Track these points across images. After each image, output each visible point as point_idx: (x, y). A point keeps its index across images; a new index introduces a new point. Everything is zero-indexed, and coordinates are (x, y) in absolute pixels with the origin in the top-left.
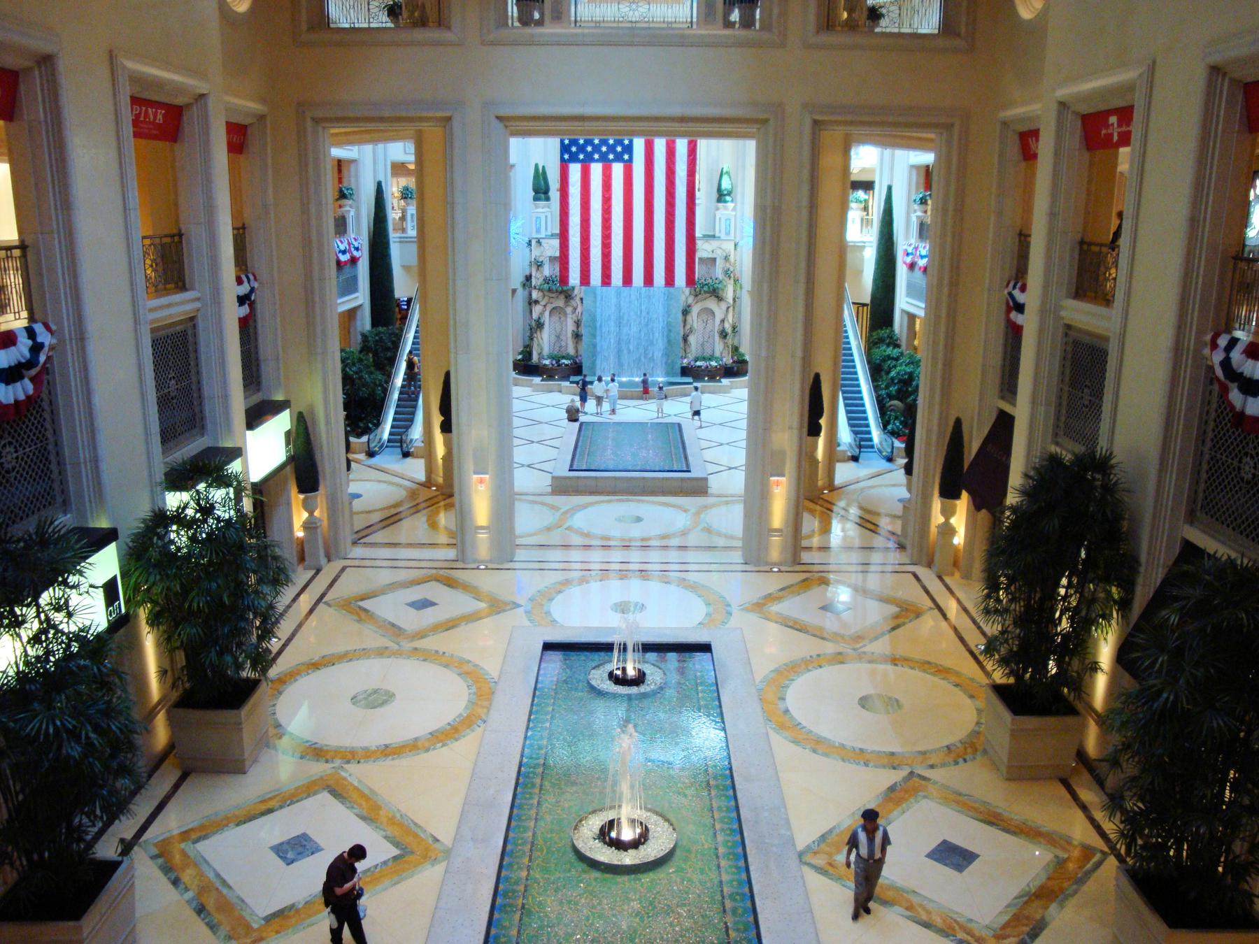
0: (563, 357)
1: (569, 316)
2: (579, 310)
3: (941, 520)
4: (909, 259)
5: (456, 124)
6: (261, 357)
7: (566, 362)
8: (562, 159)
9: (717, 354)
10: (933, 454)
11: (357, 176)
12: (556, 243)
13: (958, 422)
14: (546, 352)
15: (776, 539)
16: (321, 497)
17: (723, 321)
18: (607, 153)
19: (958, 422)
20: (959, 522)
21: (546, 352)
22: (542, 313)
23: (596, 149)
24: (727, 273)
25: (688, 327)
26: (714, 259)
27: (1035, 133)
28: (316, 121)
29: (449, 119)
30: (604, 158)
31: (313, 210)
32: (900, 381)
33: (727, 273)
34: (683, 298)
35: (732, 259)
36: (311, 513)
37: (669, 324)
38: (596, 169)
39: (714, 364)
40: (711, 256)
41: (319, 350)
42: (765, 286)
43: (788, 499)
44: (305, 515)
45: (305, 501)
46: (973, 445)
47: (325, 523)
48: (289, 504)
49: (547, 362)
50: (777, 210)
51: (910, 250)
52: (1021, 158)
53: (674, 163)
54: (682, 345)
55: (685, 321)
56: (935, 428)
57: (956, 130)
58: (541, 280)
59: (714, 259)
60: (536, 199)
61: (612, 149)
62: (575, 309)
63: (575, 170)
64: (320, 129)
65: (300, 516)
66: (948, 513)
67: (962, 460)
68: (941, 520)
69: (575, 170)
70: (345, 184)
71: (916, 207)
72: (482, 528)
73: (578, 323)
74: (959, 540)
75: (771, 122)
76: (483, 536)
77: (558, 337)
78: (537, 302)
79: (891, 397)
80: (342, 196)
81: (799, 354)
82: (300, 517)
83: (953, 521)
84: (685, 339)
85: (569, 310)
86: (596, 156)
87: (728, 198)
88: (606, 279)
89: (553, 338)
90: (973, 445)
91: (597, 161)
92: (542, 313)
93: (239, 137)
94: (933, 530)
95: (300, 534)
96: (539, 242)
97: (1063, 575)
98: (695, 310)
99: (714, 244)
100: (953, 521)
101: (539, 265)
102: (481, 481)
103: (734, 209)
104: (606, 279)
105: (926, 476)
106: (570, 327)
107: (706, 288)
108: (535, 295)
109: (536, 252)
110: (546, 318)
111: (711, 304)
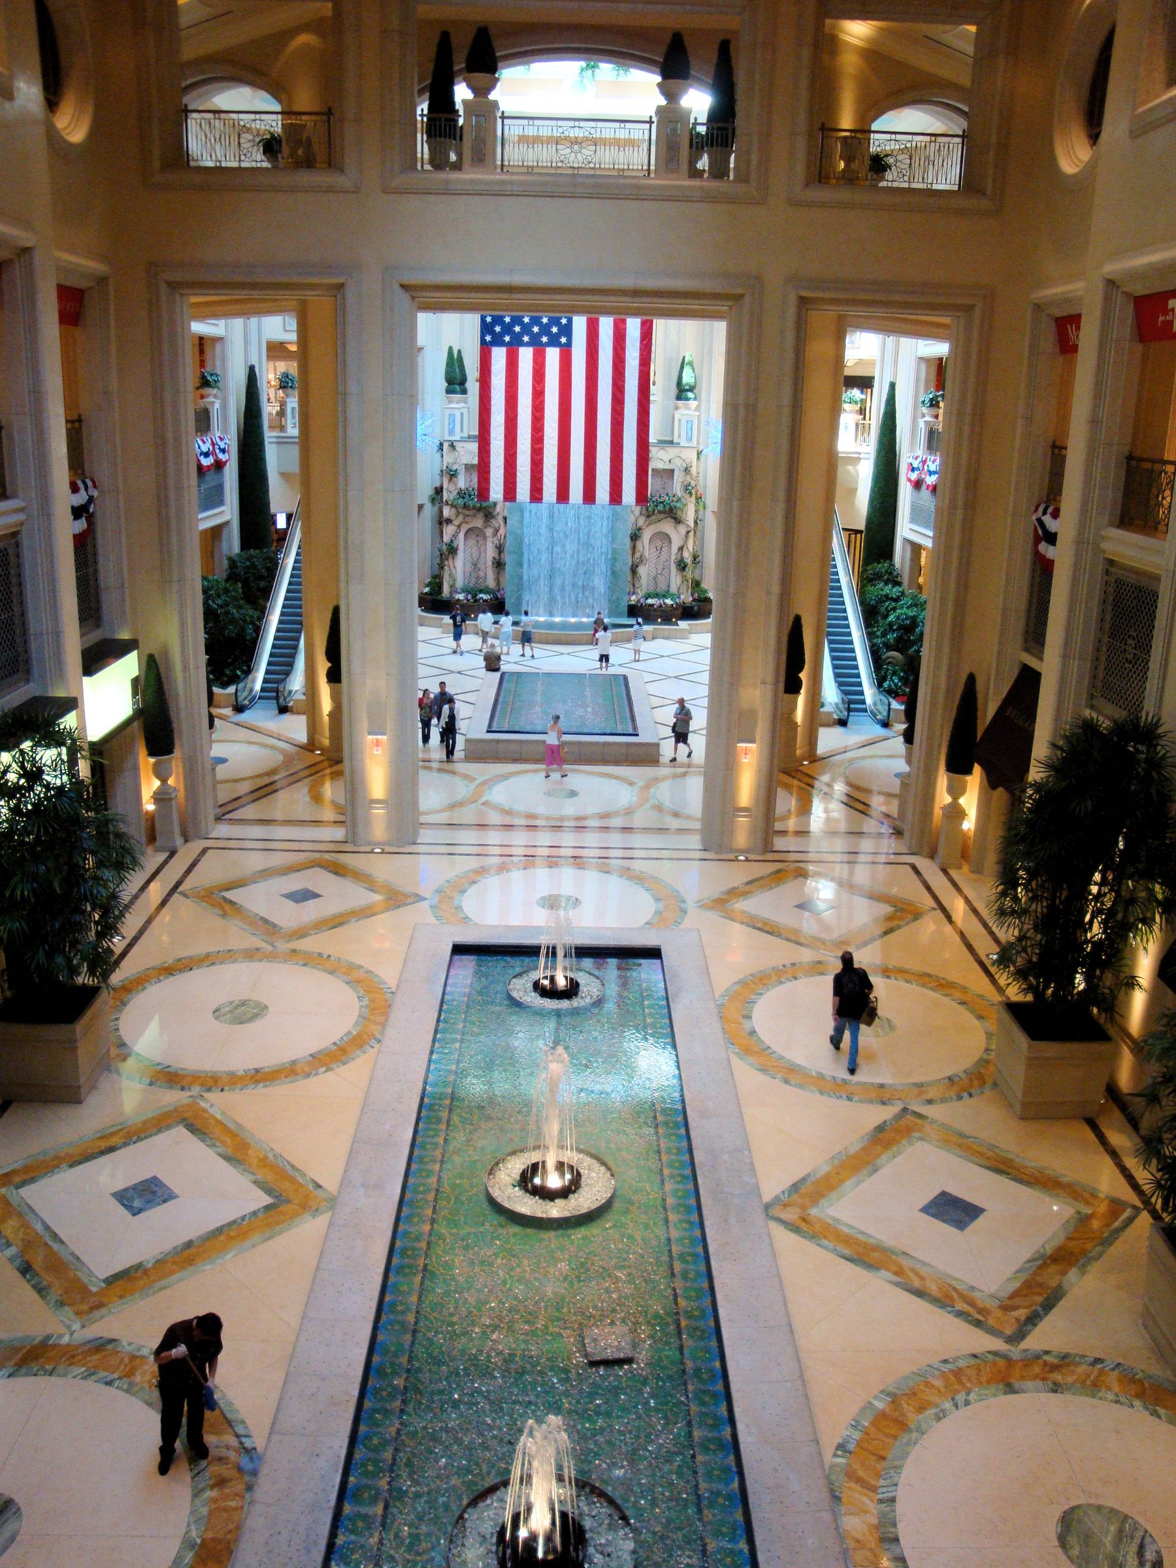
0: (481, 591)
1: (490, 540)
2: (502, 531)
3: (948, 799)
4: (914, 476)
5: (350, 294)
6: (102, 585)
7: (485, 597)
8: (483, 341)
9: (673, 589)
10: (939, 719)
11: (223, 359)
12: (474, 447)
13: (971, 680)
14: (460, 584)
15: (743, 820)
16: (176, 761)
17: (681, 549)
18: (539, 335)
19: (971, 680)
20: (970, 802)
21: (460, 584)
22: (455, 535)
23: (526, 329)
24: (687, 488)
25: (637, 555)
26: (672, 471)
27: (1075, 319)
28: (173, 286)
29: (341, 286)
30: (535, 342)
31: (168, 396)
32: (900, 627)
33: (687, 488)
34: (632, 519)
35: (694, 471)
36: (164, 781)
37: (614, 551)
38: (526, 355)
39: (669, 602)
40: (667, 467)
41: (175, 577)
42: (735, 504)
43: (759, 771)
44: (157, 783)
45: (155, 765)
46: (989, 709)
47: (181, 794)
48: (136, 768)
49: (461, 597)
50: (752, 409)
51: (915, 465)
52: (1057, 350)
53: (624, 349)
54: (629, 578)
55: (634, 548)
56: (943, 685)
57: (977, 313)
58: (455, 493)
59: (672, 471)
60: (449, 391)
61: (545, 330)
62: (497, 531)
63: (499, 356)
64: (177, 297)
65: (149, 783)
66: (956, 791)
67: (975, 728)
68: (948, 799)
69: (499, 356)
70: (209, 368)
71: (925, 410)
72: (378, 801)
73: (500, 549)
74: (969, 824)
75: (747, 300)
76: (379, 812)
78: (449, 521)
79: (888, 647)
80: (205, 383)
81: (776, 589)
82: (150, 786)
83: (962, 801)
84: (634, 570)
85: (489, 532)
86: (526, 339)
87: (690, 395)
88: (536, 493)
89: (469, 568)
90: (989, 709)
91: (527, 344)
92: (455, 535)
93: (74, 305)
94: (938, 812)
95: (150, 807)
96: (452, 446)
97: (1095, 869)
98: (646, 535)
99: (672, 452)
100: (962, 801)
101: (452, 475)
102: (377, 744)
103: (698, 408)
104: (536, 493)
105: (930, 747)
106: (490, 553)
107: (660, 507)
108: (447, 512)
109: (448, 459)
110: (460, 541)
111: (667, 527)
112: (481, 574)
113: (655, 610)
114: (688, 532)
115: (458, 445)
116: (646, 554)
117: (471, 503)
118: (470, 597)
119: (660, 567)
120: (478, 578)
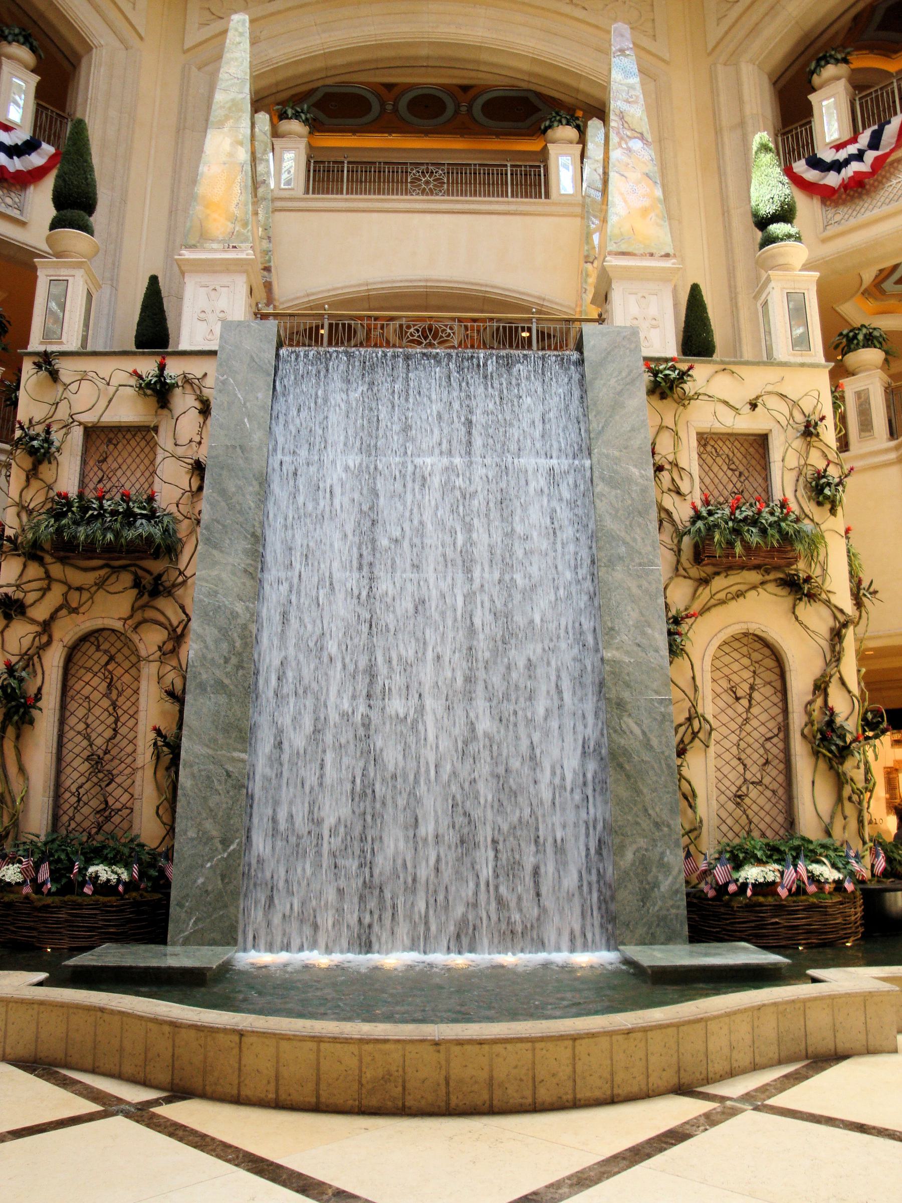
0: (95, 854)
1: (149, 671)
7: (103, 872)
9: (809, 826)
17: (821, 687)
22: (31, 658)
26: (762, 441)
40: (747, 423)
59: (762, 441)
62: (177, 637)
77: (96, 762)
89: (77, 771)
92: (31, 658)
106: (150, 711)
111: (762, 610)
112: (117, 796)
113: (780, 908)
114: (837, 635)
115: (67, 369)
116: (708, 708)
117: (82, 532)
118: (44, 873)
119: (755, 758)
120: (106, 811)
